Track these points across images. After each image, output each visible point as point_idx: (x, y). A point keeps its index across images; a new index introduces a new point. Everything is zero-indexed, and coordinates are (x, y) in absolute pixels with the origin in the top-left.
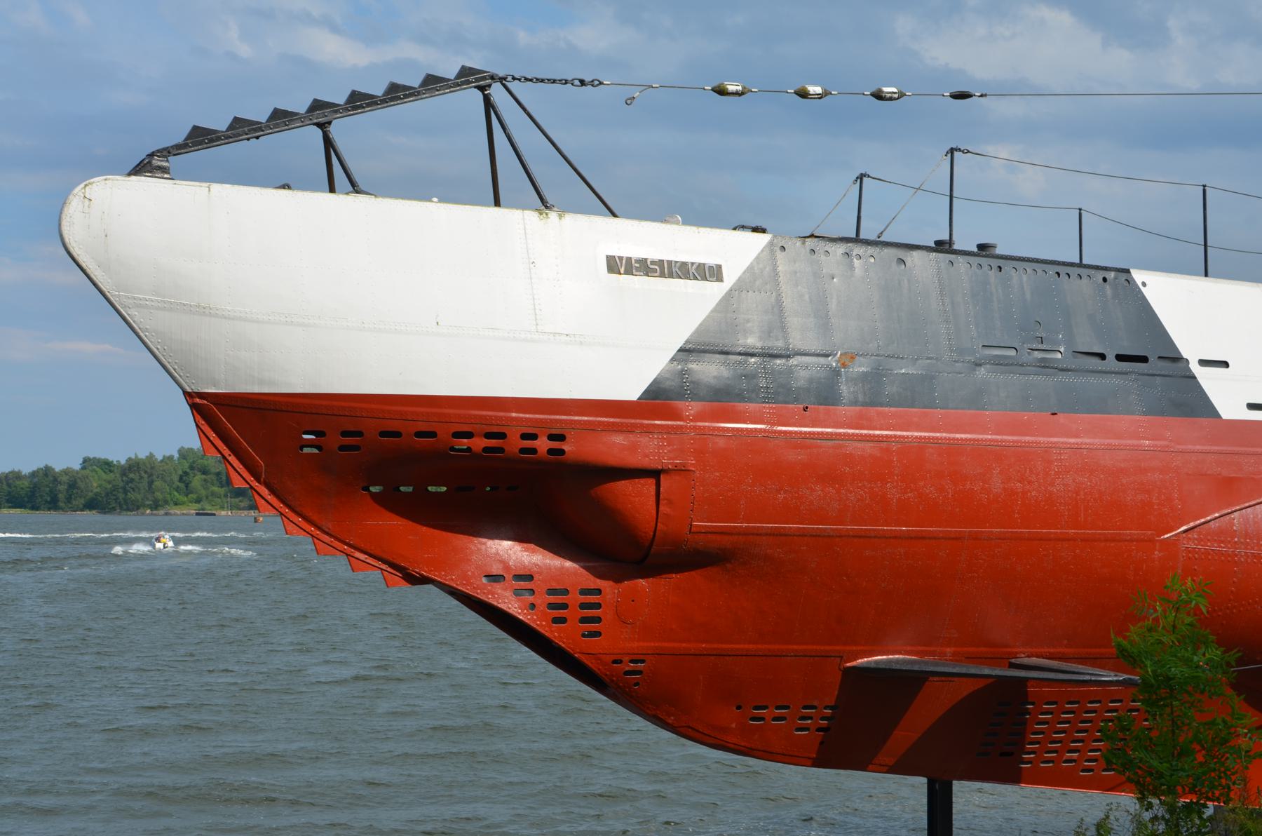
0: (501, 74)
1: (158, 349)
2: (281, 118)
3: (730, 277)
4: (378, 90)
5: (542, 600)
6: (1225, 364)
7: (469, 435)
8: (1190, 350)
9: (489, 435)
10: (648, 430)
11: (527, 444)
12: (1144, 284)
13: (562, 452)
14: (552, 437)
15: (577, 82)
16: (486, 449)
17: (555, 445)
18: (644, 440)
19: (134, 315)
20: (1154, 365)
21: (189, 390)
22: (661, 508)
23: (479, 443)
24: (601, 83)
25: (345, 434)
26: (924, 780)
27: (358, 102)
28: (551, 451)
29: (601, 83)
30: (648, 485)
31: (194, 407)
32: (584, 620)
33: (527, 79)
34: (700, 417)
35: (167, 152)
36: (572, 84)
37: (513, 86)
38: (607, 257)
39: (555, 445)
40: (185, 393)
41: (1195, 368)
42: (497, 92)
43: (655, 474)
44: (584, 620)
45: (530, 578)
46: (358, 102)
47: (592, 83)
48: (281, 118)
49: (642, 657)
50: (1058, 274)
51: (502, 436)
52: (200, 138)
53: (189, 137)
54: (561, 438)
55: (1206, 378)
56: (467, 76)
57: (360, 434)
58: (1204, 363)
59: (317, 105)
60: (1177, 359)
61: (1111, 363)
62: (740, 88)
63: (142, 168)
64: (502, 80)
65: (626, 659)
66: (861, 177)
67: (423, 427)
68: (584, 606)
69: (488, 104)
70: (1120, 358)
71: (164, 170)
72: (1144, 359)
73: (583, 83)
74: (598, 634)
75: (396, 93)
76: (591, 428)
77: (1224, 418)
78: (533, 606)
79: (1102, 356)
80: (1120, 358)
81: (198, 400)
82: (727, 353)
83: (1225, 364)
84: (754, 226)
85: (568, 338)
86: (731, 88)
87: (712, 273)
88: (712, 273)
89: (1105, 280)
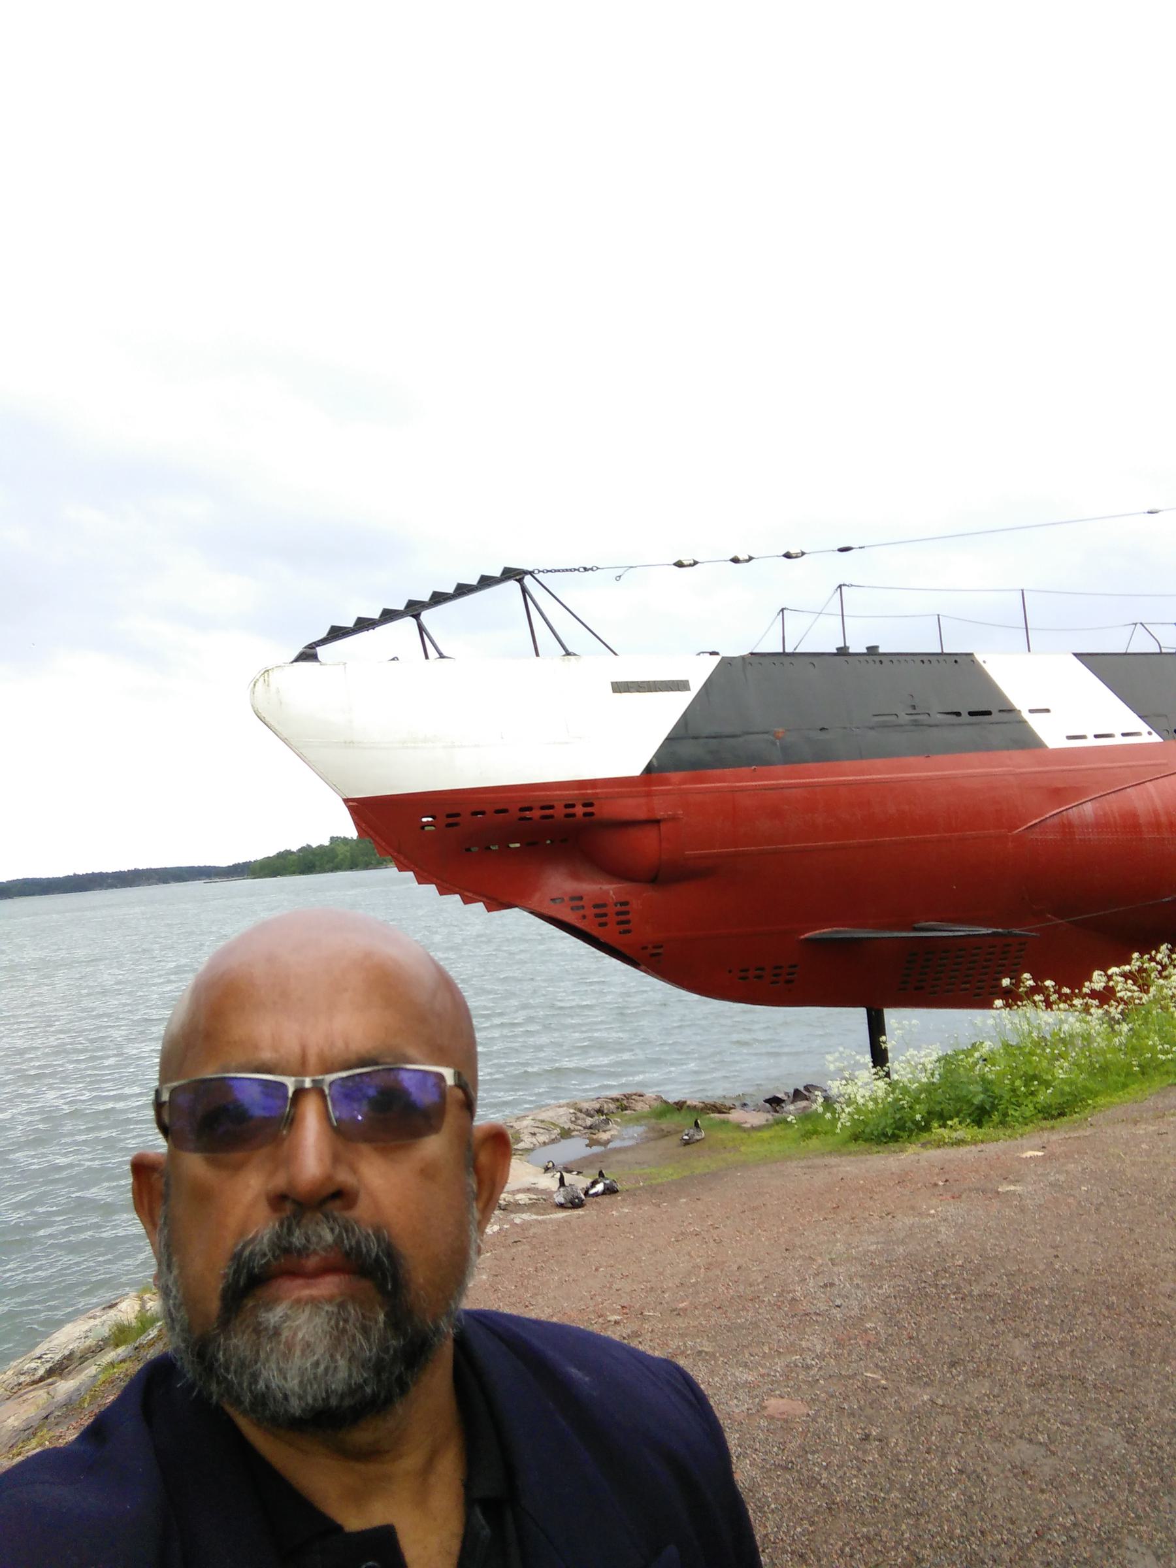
0: (530, 569)
2: (389, 615)
3: (696, 686)
4: (451, 590)
5: (590, 912)
6: (1047, 711)
7: (530, 809)
9: (543, 808)
11: (570, 811)
12: (984, 662)
14: (585, 805)
15: (582, 570)
20: (996, 716)
23: (536, 814)
25: (449, 816)
27: (438, 598)
28: (585, 814)
29: (598, 568)
33: (548, 571)
34: (684, 782)
38: (612, 683)
41: (1026, 715)
42: (528, 580)
45: (581, 898)
46: (438, 598)
47: (592, 569)
48: (389, 615)
51: (552, 807)
53: (329, 633)
55: (1034, 721)
56: (510, 574)
58: (1031, 711)
60: (1011, 710)
61: (965, 717)
64: (531, 573)
65: (650, 946)
66: (782, 610)
68: (618, 914)
69: (524, 591)
70: (971, 714)
72: (988, 713)
73: (586, 569)
74: (628, 931)
75: (463, 590)
79: (958, 714)
80: (971, 714)
81: (351, 804)
83: (1047, 711)
84: (711, 651)
88: (680, 686)
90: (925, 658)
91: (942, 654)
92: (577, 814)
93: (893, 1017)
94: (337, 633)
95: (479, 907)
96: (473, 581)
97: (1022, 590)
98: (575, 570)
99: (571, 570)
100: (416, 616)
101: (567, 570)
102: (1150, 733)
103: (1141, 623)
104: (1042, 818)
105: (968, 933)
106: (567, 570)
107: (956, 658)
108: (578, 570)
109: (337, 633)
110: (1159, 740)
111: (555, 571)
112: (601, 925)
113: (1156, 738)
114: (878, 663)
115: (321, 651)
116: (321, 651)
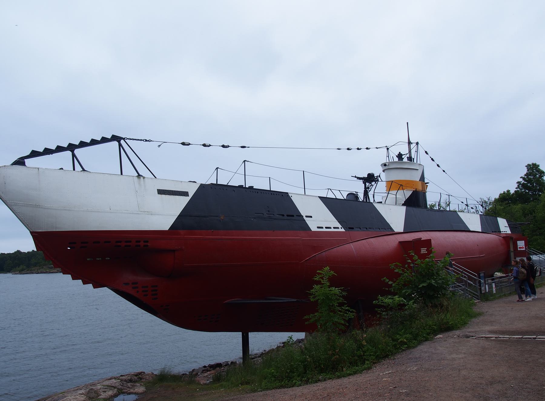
0: (124, 137)
2: (60, 149)
3: (191, 194)
4: (88, 141)
6: (311, 217)
7: (120, 242)
8: (304, 213)
9: (126, 242)
12: (291, 196)
13: (148, 246)
14: (144, 242)
15: (144, 140)
21: (32, 231)
26: (241, 333)
27: (83, 144)
28: (144, 246)
29: (151, 141)
36: (143, 141)
37: (127, 141)
40: (32, 233)
41: (304, 217)
42: (122, 142)
46: (83, 144)
47: (149, 141)
48: (60, 149)
50: (271, 194)
51: (130, 242)
53: (31, 154)
56: (115, 138)
58: (306, 216)
59: (70, 145)
61: (286, 217)
64: (124, 139)
66: (217, 168)
69: (120, 145)
70: (288, 216)
72: (293, 216)
73: (146, 141)
75: (94, 142)
79: (283, 215)
80: (288, 216)
81: (34, 234)
82: (191, 216)
83: (311, 217)
85: (148, 213)
87: (185, 194)
88: (185, 194)
91: (270, 191)
93: (251, 335)
94: (34, 154)
95: (90, 286)
96: (54, 148)
98: (142, 140)
99: (140, 140)
101: (139, 140)
102: (341, 228)
103: (330, 189)
104: (310, 257)
105: (288, 301)
106: (139, 140)
107: (282, 194)
108: (143, 140)
109: (34, 154)
111: (134, 139)
113: (343, 230)
114: (257, 192)
115: (27, 161)
116: (27, 161)
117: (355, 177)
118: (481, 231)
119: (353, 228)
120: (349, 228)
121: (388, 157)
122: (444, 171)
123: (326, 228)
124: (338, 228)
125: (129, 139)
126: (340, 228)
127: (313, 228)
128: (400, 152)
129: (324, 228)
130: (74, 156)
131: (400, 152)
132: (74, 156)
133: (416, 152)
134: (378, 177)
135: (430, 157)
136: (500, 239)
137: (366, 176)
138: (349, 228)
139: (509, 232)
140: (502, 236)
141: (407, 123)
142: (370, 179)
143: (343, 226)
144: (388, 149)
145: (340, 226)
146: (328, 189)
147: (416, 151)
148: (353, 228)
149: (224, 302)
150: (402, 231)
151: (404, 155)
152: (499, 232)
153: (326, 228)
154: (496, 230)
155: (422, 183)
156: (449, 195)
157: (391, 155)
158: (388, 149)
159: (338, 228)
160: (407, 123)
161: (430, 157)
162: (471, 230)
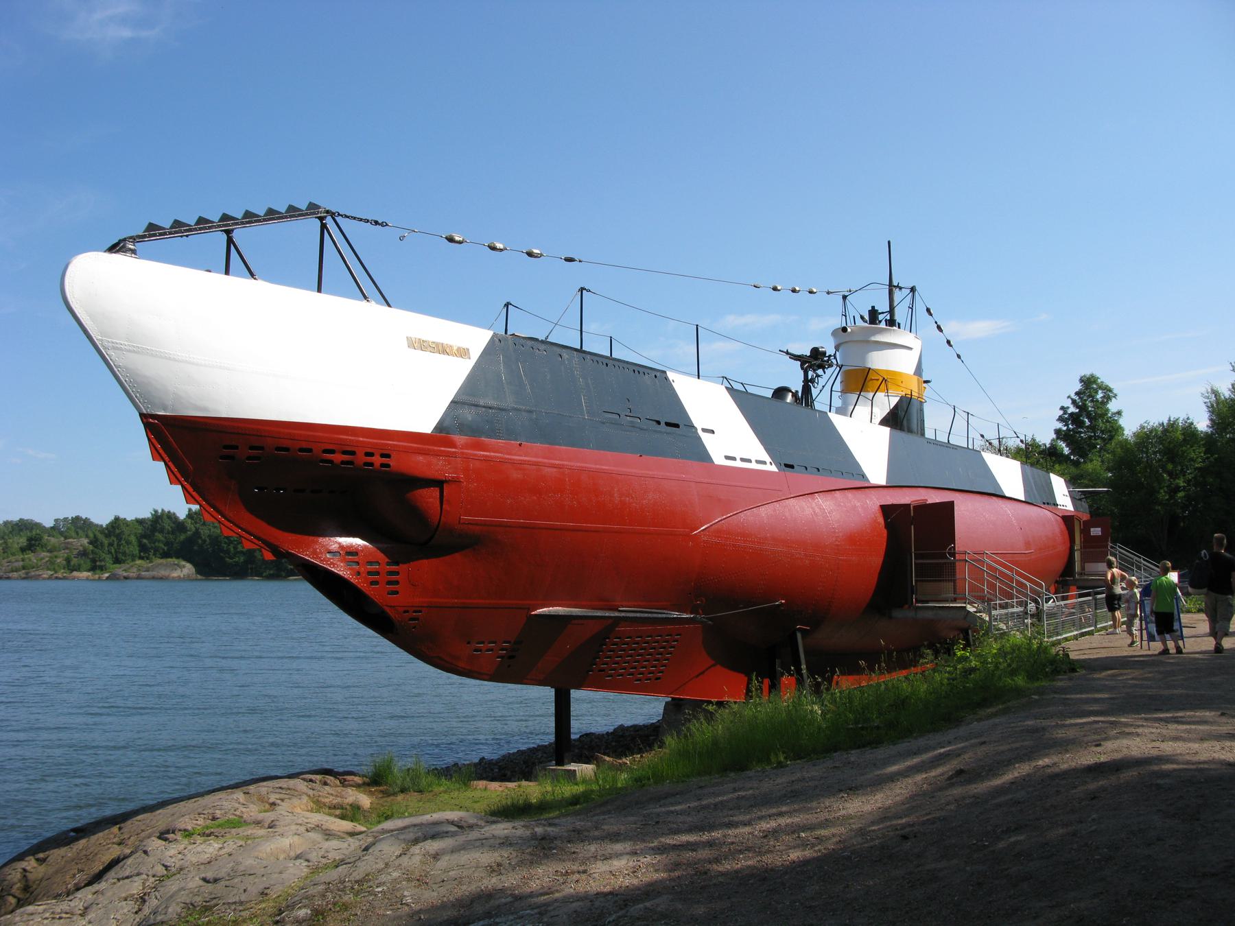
0: (334, 211)
1: (125, 381)
10: (437, 454)
11: (368, 459)
12: (673, 381)
16: (343, 462)
17: (385, 460)
18: (434, 460)
19: (112, 355)
21: (145, 412)
22: (444, 506)
23: (338, 458)
24: (387, 225)
29: (387, 225)
30: (435, 492)
31: (148, 426)
32: (390, 583)
34: (466, 446)
35: (134, 239)
37: (339, 219)
39: (385, 460)
40: (143, 416)
42: (329, 221)
43: (439, 484)
44: (390, 583)
49: (420, 609)
50: (634, 371)
51: (353, 453)
52: (153, 230)
54: (388, 456)
55: (704, 437)
56: (313, 208)
57: (262, 448)
58: (704, 430)
59: (225, 217)
60: (691, 426)
61: (663, 427)
62: (461, 239)
63: (113, 249)
64: (332, 214)
67: (304, 445)
69: (324, 227)
70: (668, 424)
71: (133, 252)
72: (677, 426)
73: (376, 223)
75: (272, 215)
76: (407, 451)
77: (716, 463)
78: (359, 573)
79: (658, 423)
80: (668, 424)
83: (713, 432)
86: (457, 239)
87: (463, 353)
88: (463, 353)
89: (656, 376)
90: (636, 369)
92: (375, 464)
97: (697, 326)
98: (368, 221)
100: (228, 232)
102: (771, 463)
110: (776, 470)
112: (372, 583)
113: (774, 468)
117: (787, 353)
118: (1024, 500)
119: (792, 467)
120: (786, 465)
121: (846, 316)
122: (959, 356)
123: (743, 460)
124: (764, 463)
125: (342, 216)
126: (768, 463)
127: (718, 459)
128: (873, 307)
129: (738, 459)
130: (230, 241)
131: (873, 307)
132: (230, 241)
133: (910, 310)
134: (831, 358)
135: (936, 323)
136: (1057, 520)
137: (809, 354)
138: (786, 465)
139: (1070, 507)
140: (1060, 515)
141: (889, 242)
142: (815, 361)
143: (775, 460)
144: (845, 297)
145: (768, 459)
146: (723, 377)
147: (911, 306)
148: (792, 467)
149: (533, 613)
150: (883, 482)
151: (883, 313)
152: (1054, 505)
153: (743, 460)
154: (1050, 502)
155: (918, 380)
156: (968, 413)
157: (851, 312)
158: (845, 297)
159: (764, 463)
160: (889, 242)
161: (936, 323)
162: (1007, 495)
